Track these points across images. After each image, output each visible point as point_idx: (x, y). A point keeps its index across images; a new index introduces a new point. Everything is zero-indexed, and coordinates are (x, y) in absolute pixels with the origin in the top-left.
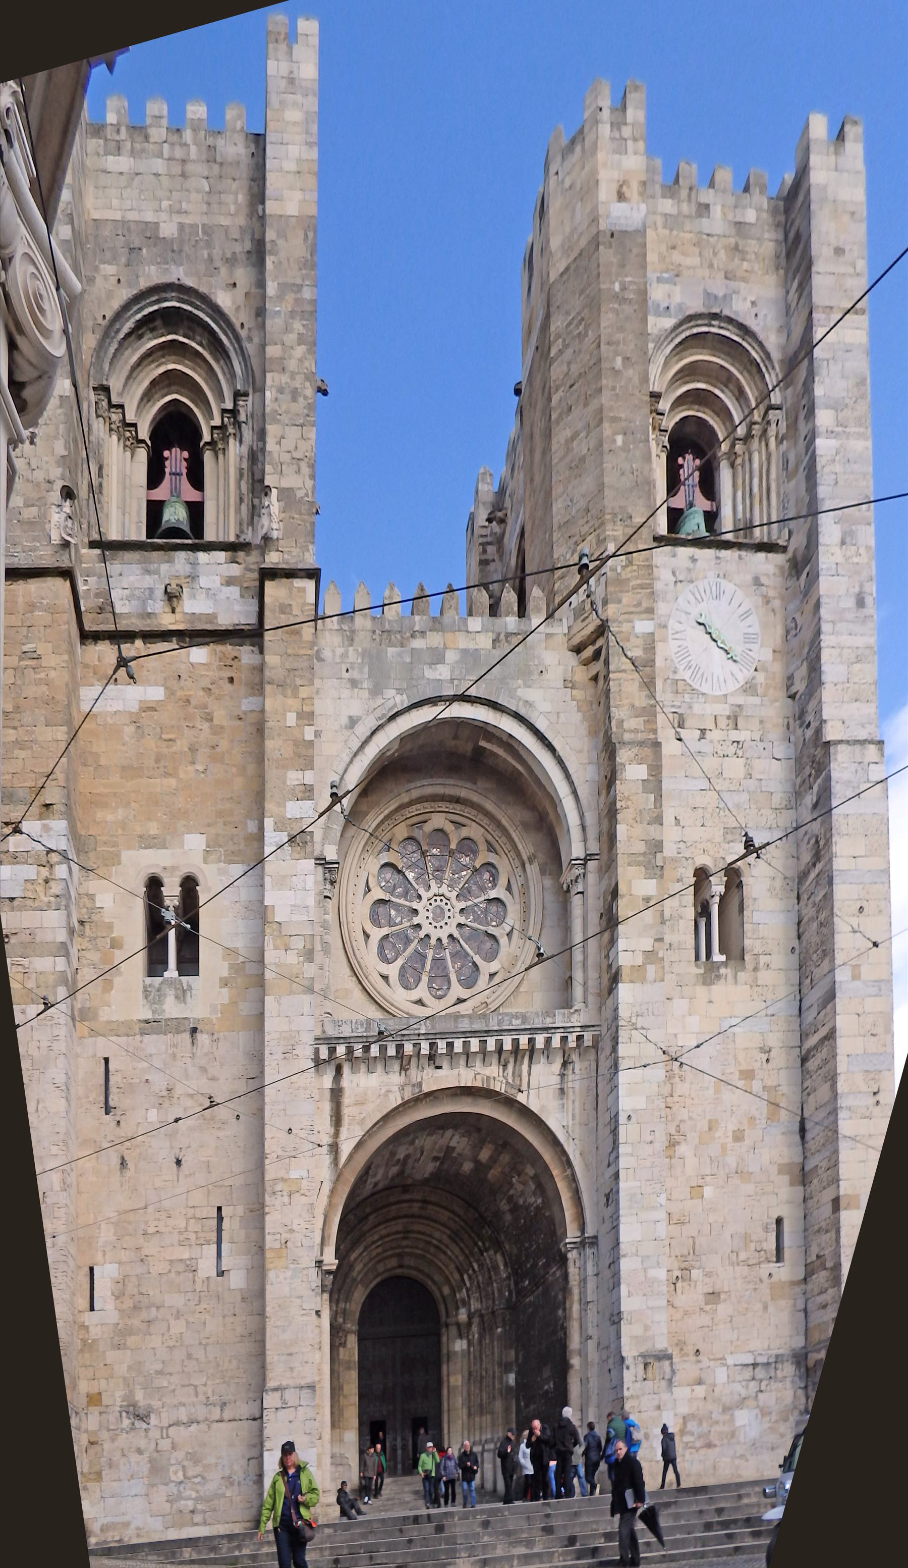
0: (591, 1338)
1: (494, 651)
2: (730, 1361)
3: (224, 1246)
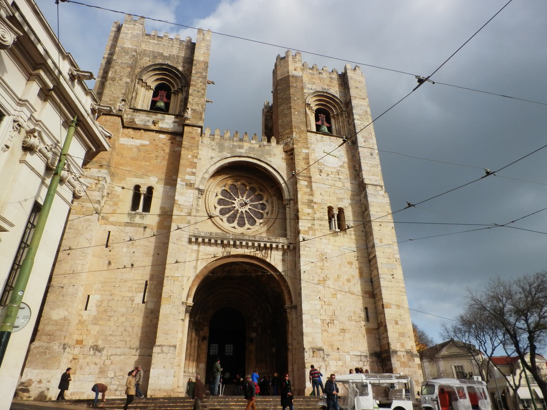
0: (295, 339)
1: (259, 149)
2: (351, 354)
3: (146, 294)
